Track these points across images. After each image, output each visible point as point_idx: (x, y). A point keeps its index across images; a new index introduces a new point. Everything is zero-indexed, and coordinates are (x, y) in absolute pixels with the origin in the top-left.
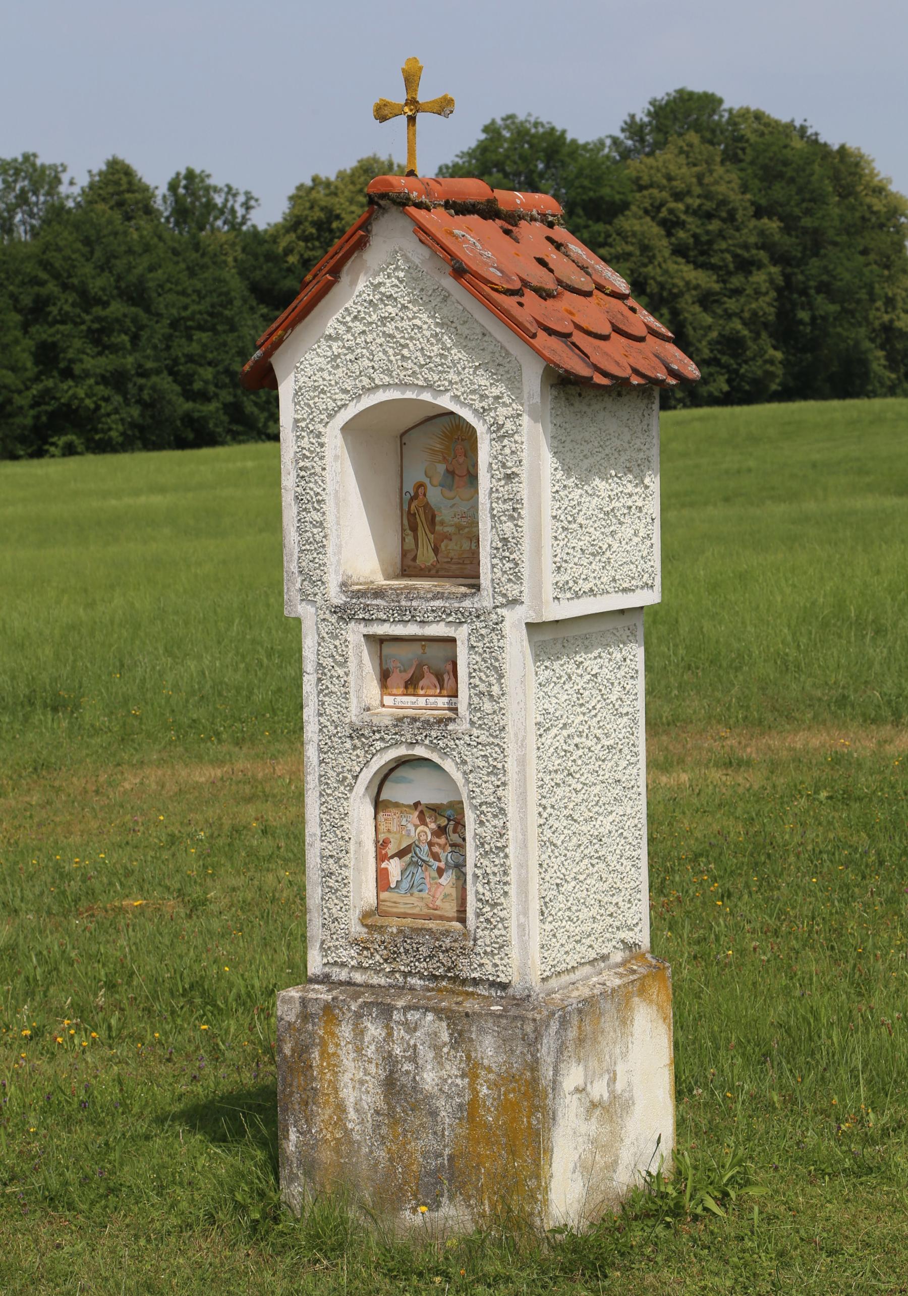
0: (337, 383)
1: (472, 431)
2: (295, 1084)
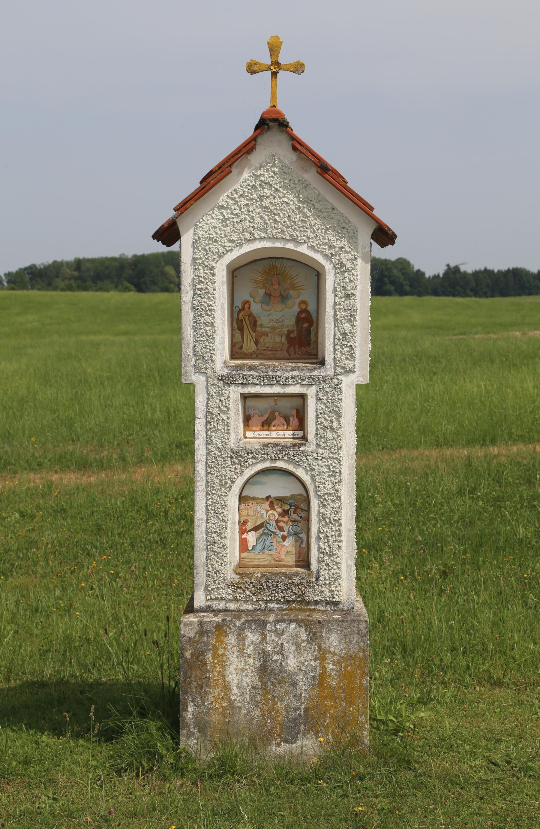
0: (226, 236)
2: (193, 676)
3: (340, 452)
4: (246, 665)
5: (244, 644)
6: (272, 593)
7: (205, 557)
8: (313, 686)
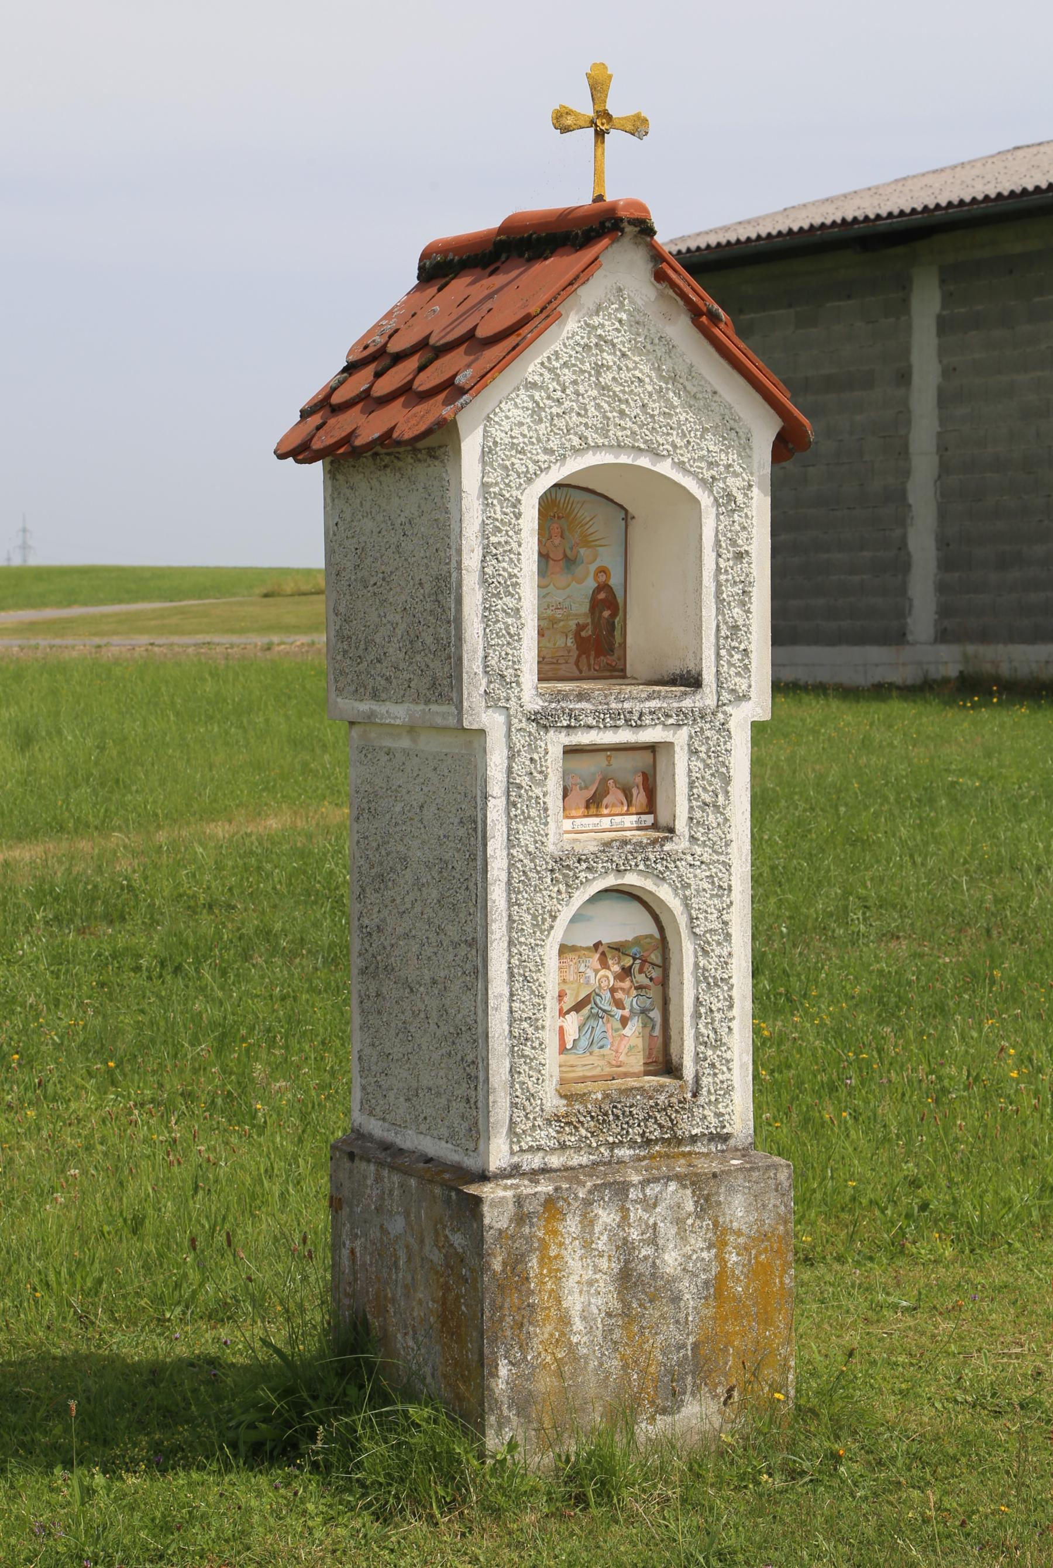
0: (539, 440)
1: (696, 502)
2: (506, 1305)
3: (729, 851)
4: (595, 1273)
5: (592, 1233)
6: (623, 1129)
7: (508, 1069)
8: (706, 1298)
